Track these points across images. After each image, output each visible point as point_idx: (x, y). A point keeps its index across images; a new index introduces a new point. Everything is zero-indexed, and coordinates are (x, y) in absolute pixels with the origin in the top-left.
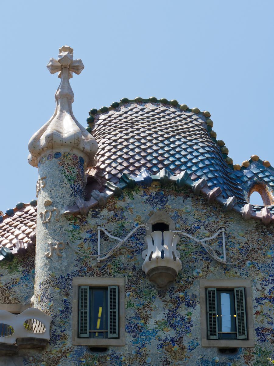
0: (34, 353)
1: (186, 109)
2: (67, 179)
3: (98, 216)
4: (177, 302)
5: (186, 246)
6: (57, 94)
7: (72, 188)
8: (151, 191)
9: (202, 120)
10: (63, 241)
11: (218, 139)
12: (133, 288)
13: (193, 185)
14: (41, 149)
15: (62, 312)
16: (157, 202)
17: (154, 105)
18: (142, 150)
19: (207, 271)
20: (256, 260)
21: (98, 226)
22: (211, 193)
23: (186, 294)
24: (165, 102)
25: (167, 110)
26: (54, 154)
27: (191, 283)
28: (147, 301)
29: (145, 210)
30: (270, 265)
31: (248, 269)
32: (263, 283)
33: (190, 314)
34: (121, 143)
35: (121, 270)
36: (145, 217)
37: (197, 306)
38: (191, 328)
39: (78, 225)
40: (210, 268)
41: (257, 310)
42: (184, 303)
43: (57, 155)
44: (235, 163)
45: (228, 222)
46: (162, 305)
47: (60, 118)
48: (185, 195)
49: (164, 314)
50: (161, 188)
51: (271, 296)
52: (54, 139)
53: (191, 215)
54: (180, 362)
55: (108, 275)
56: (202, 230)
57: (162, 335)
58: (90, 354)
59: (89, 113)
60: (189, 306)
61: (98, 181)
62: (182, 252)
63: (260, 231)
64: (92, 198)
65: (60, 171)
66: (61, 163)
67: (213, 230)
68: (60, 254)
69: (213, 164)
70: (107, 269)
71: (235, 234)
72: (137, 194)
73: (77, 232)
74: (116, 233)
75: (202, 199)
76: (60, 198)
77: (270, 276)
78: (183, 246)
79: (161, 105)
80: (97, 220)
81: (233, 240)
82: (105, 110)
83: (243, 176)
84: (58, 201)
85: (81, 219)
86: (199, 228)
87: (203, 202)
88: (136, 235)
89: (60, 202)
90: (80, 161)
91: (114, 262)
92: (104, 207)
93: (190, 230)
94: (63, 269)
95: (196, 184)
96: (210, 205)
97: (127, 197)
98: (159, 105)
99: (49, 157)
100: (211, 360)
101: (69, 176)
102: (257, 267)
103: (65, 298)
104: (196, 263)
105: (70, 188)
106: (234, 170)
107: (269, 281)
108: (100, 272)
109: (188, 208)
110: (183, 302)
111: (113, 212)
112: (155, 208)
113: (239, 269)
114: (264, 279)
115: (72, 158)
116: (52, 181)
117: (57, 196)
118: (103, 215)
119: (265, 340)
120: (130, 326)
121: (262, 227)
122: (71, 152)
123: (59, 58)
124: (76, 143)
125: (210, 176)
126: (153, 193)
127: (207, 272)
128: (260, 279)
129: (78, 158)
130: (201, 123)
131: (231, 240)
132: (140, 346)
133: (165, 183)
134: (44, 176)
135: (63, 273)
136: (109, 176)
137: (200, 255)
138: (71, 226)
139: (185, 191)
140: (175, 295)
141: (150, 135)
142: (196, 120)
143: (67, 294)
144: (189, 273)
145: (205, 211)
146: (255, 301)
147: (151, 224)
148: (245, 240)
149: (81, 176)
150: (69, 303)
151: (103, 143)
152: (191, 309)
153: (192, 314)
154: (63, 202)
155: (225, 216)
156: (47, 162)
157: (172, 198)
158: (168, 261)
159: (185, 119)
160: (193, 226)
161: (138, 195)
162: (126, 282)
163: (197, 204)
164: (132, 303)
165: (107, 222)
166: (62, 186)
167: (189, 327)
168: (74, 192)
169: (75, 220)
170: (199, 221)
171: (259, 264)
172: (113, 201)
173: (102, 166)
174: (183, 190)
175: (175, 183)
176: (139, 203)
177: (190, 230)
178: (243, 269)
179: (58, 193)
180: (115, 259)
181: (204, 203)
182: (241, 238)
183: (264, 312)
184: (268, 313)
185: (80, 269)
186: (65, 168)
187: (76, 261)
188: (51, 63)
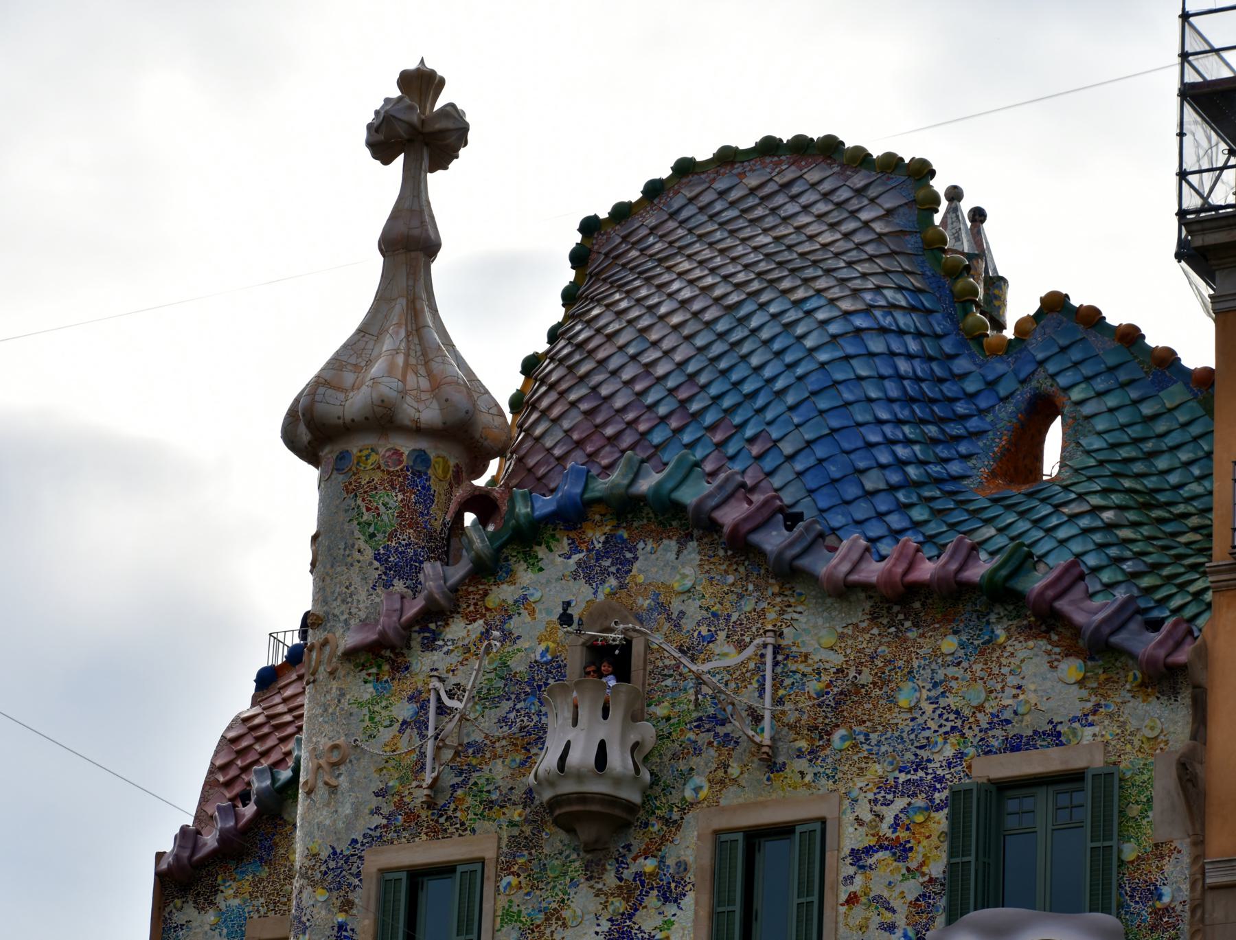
4: (634, 892)
5: (673, 705)
8: (590, 533)
10: (343, 738)
12: (521, 861)
20: (864, 722)
21: (433, 679)
23: (662, 861)
27: (677, 825)
28: (558, 898)
30: (905, 735)
31: (838, 757)
32: (879, 796)
33: (668, 924)
35: (491, 808)
37: (686, 899)
39: (386, 682)
40: (730, 770)
41: (852, 889)
42: (655, 892)
45: (790, 606)
46: (593, 905)
49: (597, 933)
51: (898, 837)
55: (457, 829)
56: (721, 645)
60: (666, 900)
63: (885, 622)
66: (350, 484)
67: (748, 640)
68: (333, 782)
70: (455, 810)
71: (809, 644)
72: (551, 550)
73: (384, 704)
74: (485, 691)
76: (343, 601)
77: (901, 771)
78: (666, 704)
81: (802, 667)
85: (394, 661)
86: (712, 639)
88: (539, 687)
89: (342, 613)
91: (475, 784)
93: (689, 649)
94: (341, 825)
101: (370, 525)
102: (865, 747)
103: (341, 918)
104: (694, 758)
105: (371, 564)
107: (896, 787)
108: (437, 821)
110: (652, 889)
111: (481, 622)
113: (810, 761)
118: (449, 636)
121: (889, 609)
126: (597, 537)
127: (722, 782)
128: (871, 785)
131: (793, 668)
135: (338, 839)
137: (708, 731)
138: (370, 688)
139: (680, 519)
140: (634, 869)
143: (346, 906)
144: (674, 792)
145: (731, 579)
146: (849, 860)
147: (583, 644)
148: (837, 659)
150: (352, 930)
152: (671, 909)
153: (673, 923)
154: (350, 613)
157: (649, 548)
160: (696, 634)
162: (503, 845)
164: (515, 909)
166: (349, 560)
168: (385, 574)
169: (379, 667)
170: (714, 615)
171: (872, 736)
176: (557, 580)
177: (689, 649)
178: (823, 760)
180: (478, 774)
181: (730, 553)
182: (824, 654)
183: (872, 894)
184: (886, 894)
185: (385, 822)
186: (359, 501)
187: (377, 795)
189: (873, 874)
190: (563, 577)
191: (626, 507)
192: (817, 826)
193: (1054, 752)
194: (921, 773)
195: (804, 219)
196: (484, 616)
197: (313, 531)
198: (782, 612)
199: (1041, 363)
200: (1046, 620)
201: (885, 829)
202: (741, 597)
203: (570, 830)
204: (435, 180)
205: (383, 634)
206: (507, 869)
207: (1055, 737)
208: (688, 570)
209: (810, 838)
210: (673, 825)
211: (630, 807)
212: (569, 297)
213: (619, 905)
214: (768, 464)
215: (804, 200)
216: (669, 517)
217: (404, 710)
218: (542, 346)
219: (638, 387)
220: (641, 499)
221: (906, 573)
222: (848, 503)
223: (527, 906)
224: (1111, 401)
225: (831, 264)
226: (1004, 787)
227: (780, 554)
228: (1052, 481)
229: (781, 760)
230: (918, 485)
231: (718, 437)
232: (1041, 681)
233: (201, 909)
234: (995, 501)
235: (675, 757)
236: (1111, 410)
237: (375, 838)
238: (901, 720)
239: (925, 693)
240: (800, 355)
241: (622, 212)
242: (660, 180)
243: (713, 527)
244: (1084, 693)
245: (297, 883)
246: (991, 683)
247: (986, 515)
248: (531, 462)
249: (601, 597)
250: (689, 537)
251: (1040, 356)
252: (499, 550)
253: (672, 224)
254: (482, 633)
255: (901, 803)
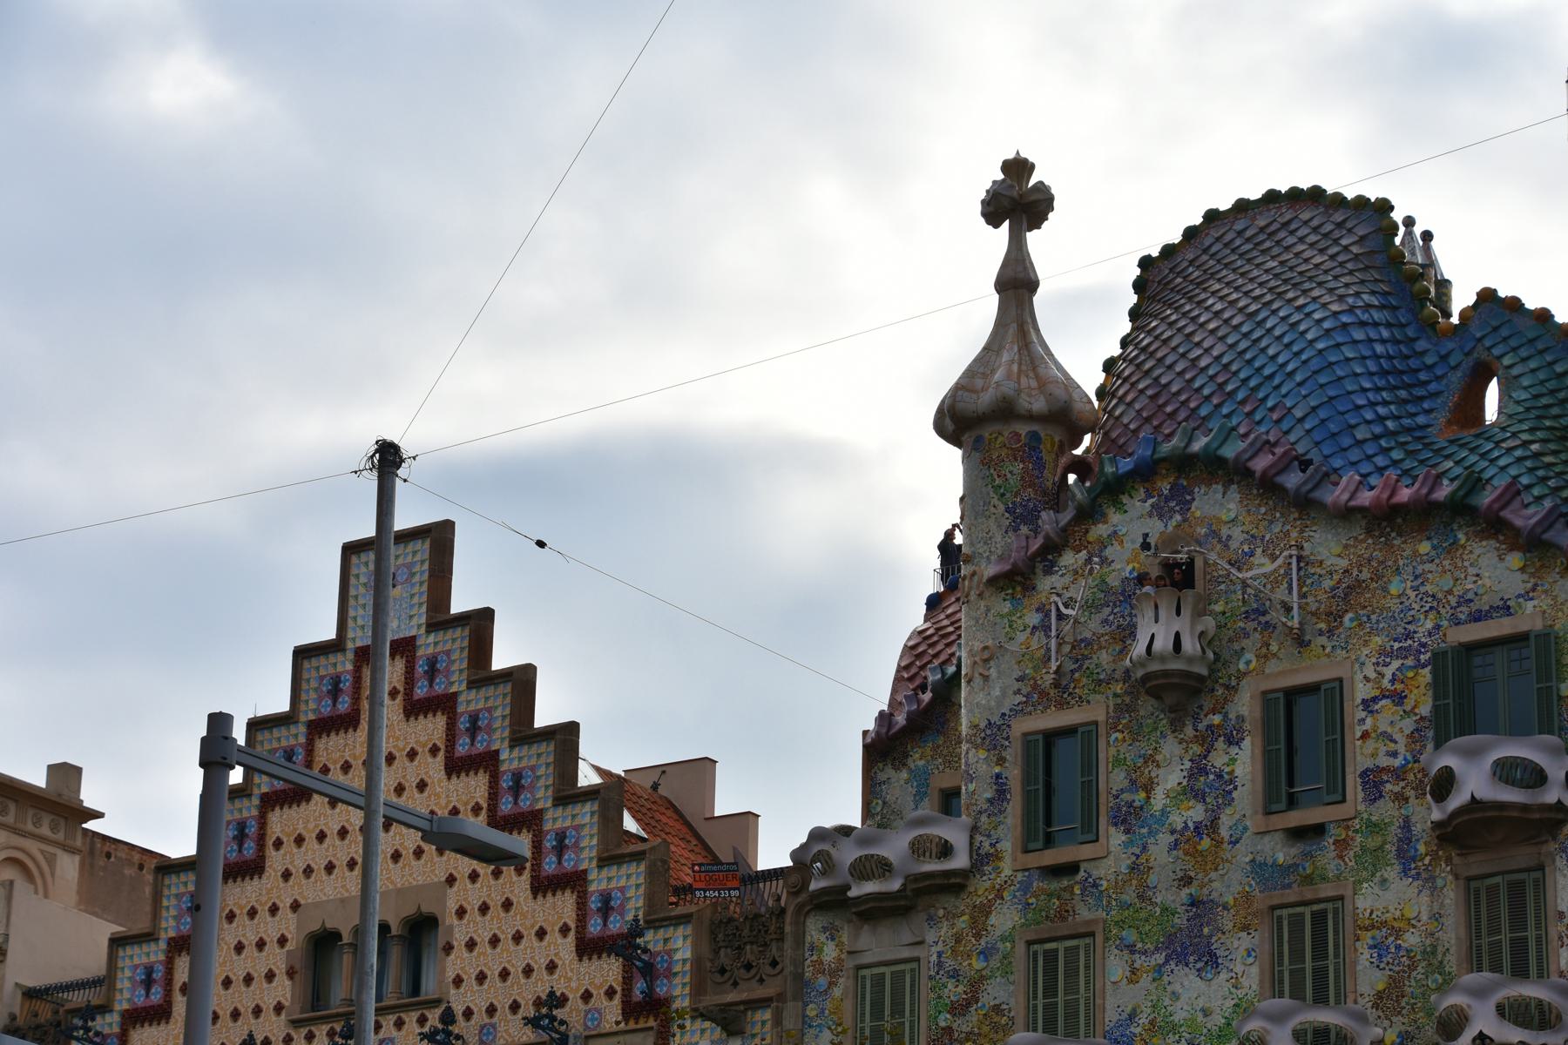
0: (949, 901)
1: (1338, 200)
4: (1207, 739)
15: (990, 801)
19: (1264, 657)
23: (1226, 716)
27: (1235, 689)
38: (1235, 794)
46: (1177, 750)
54: (1213, 875)
56: (1259, 558)
57: (1177, 820)
58: (1044, 885)
60: (1230, 743)
62: (1220, 618)
80: (1054, 578)
86: (1252, 554)
100: (1270, 861)
103: (997, 770)
114: (1382, 652)
119: (1381, 796)
120: (1119, 809)
126: (1165, 486)
127: (1265, 656)
132: (1138, 851)
138: (1008, 604)
143: (1001, 761)
145: (1263, 510)
148: (1344, 563)
152: (1234, 750)
158: (1162, 658)
167: (1230, 792)
184: (1389, 730)
189: (1379, 716)
191: (1184, 464)
192: (1337, 684)
193: (1506, 621)
194: (1410, 642)
195: (1301, 247)
197: (961, 494)
198: (1302, 531)
199: (1480, 340)
200: (1494, 526)
201: (1386, 683)
202: (1271, 522)
203: (1158, 698)
204: (1033, 238)
205: (1014, 565)
206: (1115, 728)
207: (1506, 609)
208: (1232, 506)
209: (1331, 693)
210: (1232, 689)
211: (1200, 678)
212: (1134, 314)
213: (1197, 749)
214: (1285, 426)
215: (1300, 233)
216: (1214, 468)
217: (1034, 619)
218: (1117, 351)
219: (1188, 376)
220: (1195, 456)
221: (1391, 496)
222: (1345, 450)
223: (1130, 754)
224: (1533, 364)
225: (1322, 278)
226: (1471, 648)
227: (1298, 489)
228: (1493, 425)
229: (1307, 638)
230: (1394, 434)
231: (1247, 409)
232: (1493, 571)
233: (897, 769)
234: (1452, 442)
235: (1230, 640)
236: (1533, 371)
237: (1017, 711)
238: (1393, 604)
239: (1409, 584)
240: (1303, 345)
241: (1168, 250)
242: (1195, 227)
243: (1249, 473)
244: (1525, 577)
245: (964, 747)
246: (1457, 574)
247: (1446, 453)
248: (1114, 435)
249: (1170, 528)
250: (1231, 482)
251: (1478, 335)
252: (1094, 500)
253: (1205, 257)
255: (1396, 664)
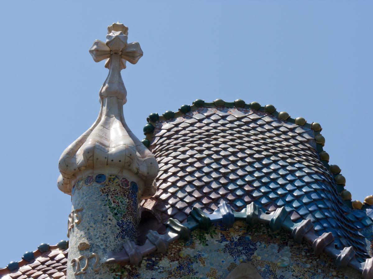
1: (287, 119)
2: (112, 213)
3: (154, 267)
6: (103, 91)
7: (119, 226)
8: (232, 234)
9: (310, 135)
11: (330, 163)
13: (293, 228)
14: (77, 169)
16: (240, 251)
17: (241, 111)
18: (221, 175)
22: (319, 240)
24: (256, 108)
25: (260, 119)
26: (95, 176)
29: (223, 262)
34: (192, 164)
36: (223, 272)
43: (100, 178)
44: (355, 198)
47: (107, 125)
48: (282, 242)
50: (247, 230)
52: (96, 155)
53: (289, 271)
59: (148, 120)
61: (156, 217)
64: (147, 241)
65: (102, 201)
66: (105, 189)
69: (323, 198)
72: (212, 237)
75: (304, 248)
76: (102, 240)
79: (251, 112)
80: (154, 273)
82: (170, 117)
83: (365, 217)
84: (98, 244)
85: (130, 271)
87: (306, 253)
89: (102, 245)
90: (132, 187)
92: (164, 255)
95: (298, 226)
96: (316, 257)
97: (197, 242)
98: (248, 112)
99: (88, 180)
101: (115, 209)
105: (116, 226)
106: (352, 208)
109: (285, 261)
111: (177, 262)
112: (238, 259)
115: (120, 183)
116: (91, 215)
117: (98, 236)
122: (119, 175)
123: (107, 40)
124: (127, 162)
125: (318, 216)
126: (236, 236)
129: (130, 183)
130: (308, 139)
133: (253, 223)
134: (79, 208)
136: (172, 211)
141: (234, 154)
142: (300, 135)
145: (309, 266)
149: (132, 209)
151: (166, 164)
154: (106, 246)
155: (337, 273)
156: (85, 187)
157: (263, 245)
159: (285, 133)
161: (214, 240)
163: (298, 256)
165: (167, 276)
166: (105, 222)
168: (122, 232)
169: (122, 272)
172: (178, 246)
173: (164, 196)
174: (278, 234)
175: (267, 224)
176: (215, 251)
179: (99, 233)
186: (110, 198)
188: (95, 47)
190: (218, 250)
196: (178, 260)
254: (178, 267)
